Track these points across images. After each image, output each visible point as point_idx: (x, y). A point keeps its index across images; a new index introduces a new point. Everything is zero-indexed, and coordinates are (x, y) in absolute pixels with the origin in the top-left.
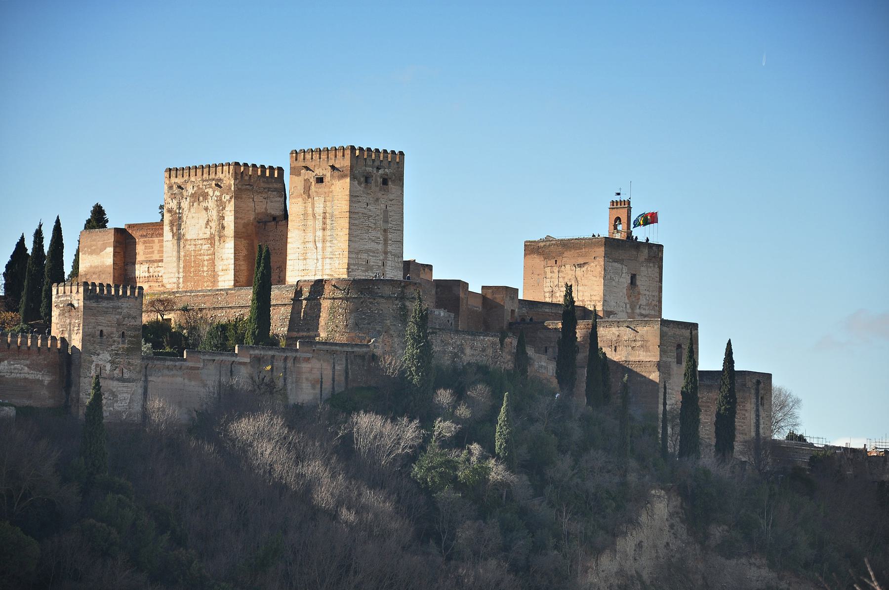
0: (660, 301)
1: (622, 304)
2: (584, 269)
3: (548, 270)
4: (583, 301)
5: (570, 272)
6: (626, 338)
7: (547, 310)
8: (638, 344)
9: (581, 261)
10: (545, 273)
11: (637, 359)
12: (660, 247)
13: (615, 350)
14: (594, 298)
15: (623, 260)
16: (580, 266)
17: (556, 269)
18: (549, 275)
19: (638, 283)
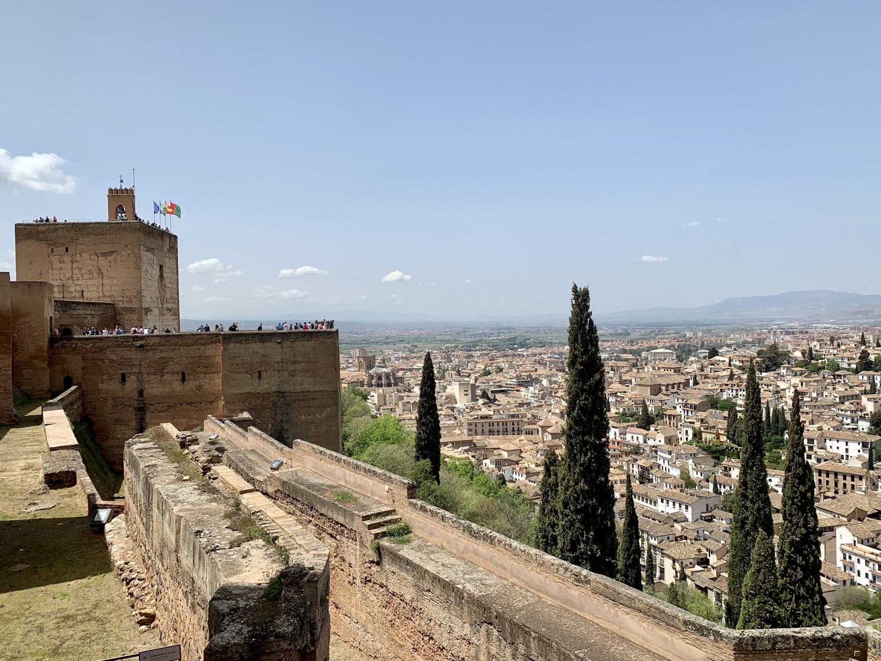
0: (178, 294)
1: (155, 299)
2: (111, 258)
3: (55, 259)
4: (110, 297)
5: (89, 262)
6: (277, 358)
7: (81, 312)
8: (299, 367)
9: (106, 248)
10: (51, 263)
11: (299, 388)
12: (176, 237)
13: (260, 377)
14: (127, 293)
15: (153, 249)
16: (105, 255)
17: (67, 259)
18: (57, 265)
19: (165, 276)
